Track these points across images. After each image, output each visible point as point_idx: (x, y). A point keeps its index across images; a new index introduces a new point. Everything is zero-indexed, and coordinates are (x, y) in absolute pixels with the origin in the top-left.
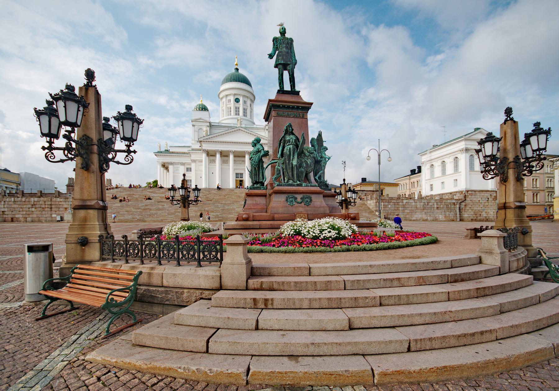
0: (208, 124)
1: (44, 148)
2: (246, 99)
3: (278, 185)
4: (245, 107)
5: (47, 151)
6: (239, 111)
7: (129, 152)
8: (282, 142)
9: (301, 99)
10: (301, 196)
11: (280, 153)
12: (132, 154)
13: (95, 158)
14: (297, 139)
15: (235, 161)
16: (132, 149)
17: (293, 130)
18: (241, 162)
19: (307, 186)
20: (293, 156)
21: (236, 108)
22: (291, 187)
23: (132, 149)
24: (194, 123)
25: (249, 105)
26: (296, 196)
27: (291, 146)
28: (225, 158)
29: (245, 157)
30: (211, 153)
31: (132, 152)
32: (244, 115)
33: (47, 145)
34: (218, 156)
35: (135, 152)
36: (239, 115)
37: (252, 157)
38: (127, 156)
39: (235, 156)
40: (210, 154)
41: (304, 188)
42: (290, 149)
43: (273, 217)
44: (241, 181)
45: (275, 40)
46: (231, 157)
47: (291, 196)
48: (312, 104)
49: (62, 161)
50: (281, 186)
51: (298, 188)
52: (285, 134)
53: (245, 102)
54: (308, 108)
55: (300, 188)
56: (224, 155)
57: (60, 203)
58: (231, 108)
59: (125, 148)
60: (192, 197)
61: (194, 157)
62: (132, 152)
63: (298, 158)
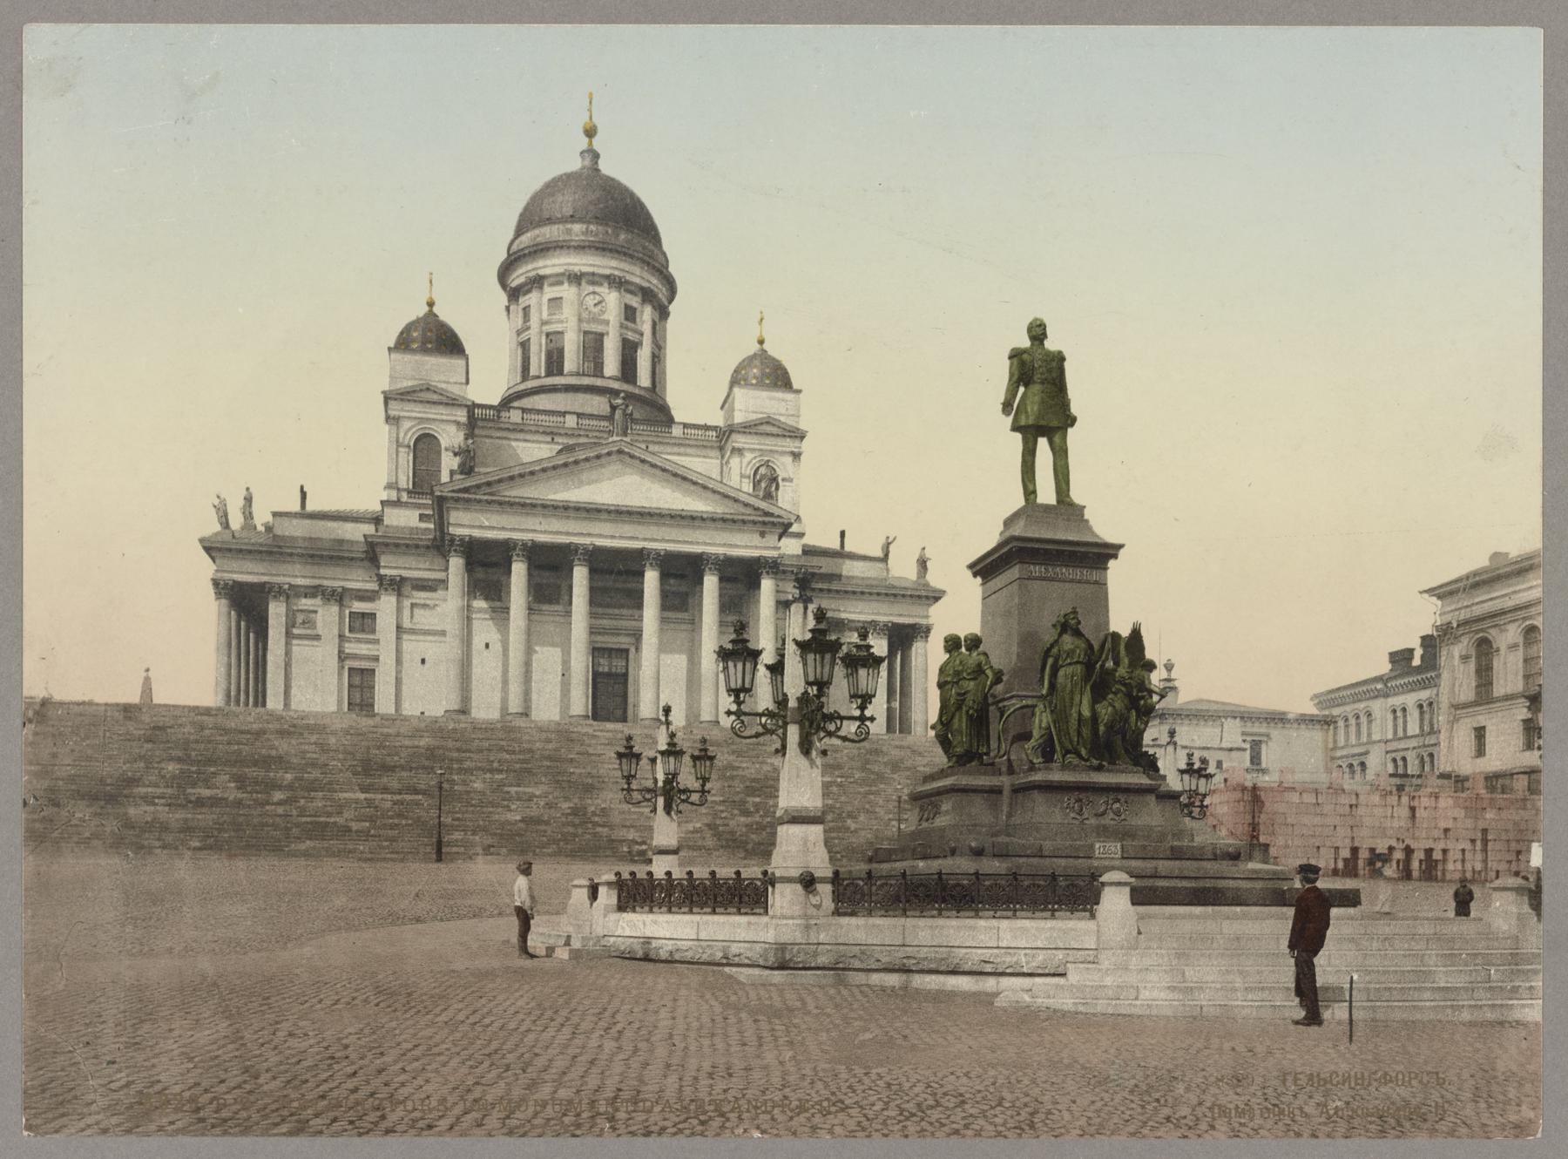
0: (462, 416)
1: (729, 713)
2: (634, 301)
5: (733, 717)
7: (862, 719)
9: (1093, 533)
14: (1091, 646)
16: (868, 713)
23: (868, 713)
24: (396, 409)
25: (647, 328)
33: (734, 708)
45: (1016, 355)
48: (1121, 546)
49: (757, 735)
52: (1060, 635)
53: (630, 314)
54: (1115, 556)
59: (857, 713)
61: (391, 566)
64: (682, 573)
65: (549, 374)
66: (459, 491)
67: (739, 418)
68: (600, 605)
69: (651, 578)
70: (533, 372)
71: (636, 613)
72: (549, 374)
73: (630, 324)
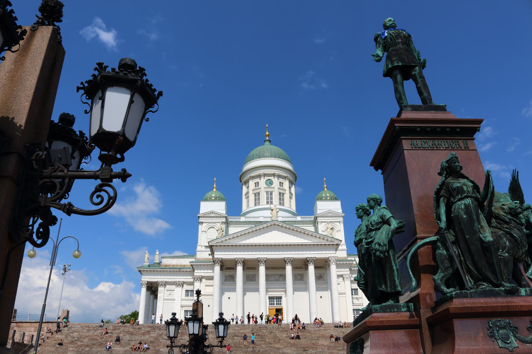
2: (281, 180)
3: (458, 296)
4: (281, 191)
6: (271, 198)
11: (444, 218)
12: (116, 182)
14: (476, 187)
15: (267, 276)
17: (461, 168)
18: (277, 277)
20: (479, 223)
22: (493, 299)
26: (515, 321)
27: (468, 201)
28: (251, 272)
29: (284, 268)
30: (227, 265)
31: (117, 176)
32: (280, 204)
34: (240, 269)
35: (124, 176)
36: (272, 203)
37: (361, 240)
38: (99, 189)
39: (267, 268)
40: (228, 267)
42: (467, 206)
44: (279, 311)
46: (262, 269)
50: (466, 296)
51: (509, 299)
53: (281, 184)
56: (250, 267)
58: (259, 193)
60: (211, 339)
62: (117, 176)
64: (301, 266)
65: (255, 205)
66: (219, 243)
68: (271, 281)
69: (289, 268)
70: (250, 206)
71: (284, 282)
72: (255, 205)
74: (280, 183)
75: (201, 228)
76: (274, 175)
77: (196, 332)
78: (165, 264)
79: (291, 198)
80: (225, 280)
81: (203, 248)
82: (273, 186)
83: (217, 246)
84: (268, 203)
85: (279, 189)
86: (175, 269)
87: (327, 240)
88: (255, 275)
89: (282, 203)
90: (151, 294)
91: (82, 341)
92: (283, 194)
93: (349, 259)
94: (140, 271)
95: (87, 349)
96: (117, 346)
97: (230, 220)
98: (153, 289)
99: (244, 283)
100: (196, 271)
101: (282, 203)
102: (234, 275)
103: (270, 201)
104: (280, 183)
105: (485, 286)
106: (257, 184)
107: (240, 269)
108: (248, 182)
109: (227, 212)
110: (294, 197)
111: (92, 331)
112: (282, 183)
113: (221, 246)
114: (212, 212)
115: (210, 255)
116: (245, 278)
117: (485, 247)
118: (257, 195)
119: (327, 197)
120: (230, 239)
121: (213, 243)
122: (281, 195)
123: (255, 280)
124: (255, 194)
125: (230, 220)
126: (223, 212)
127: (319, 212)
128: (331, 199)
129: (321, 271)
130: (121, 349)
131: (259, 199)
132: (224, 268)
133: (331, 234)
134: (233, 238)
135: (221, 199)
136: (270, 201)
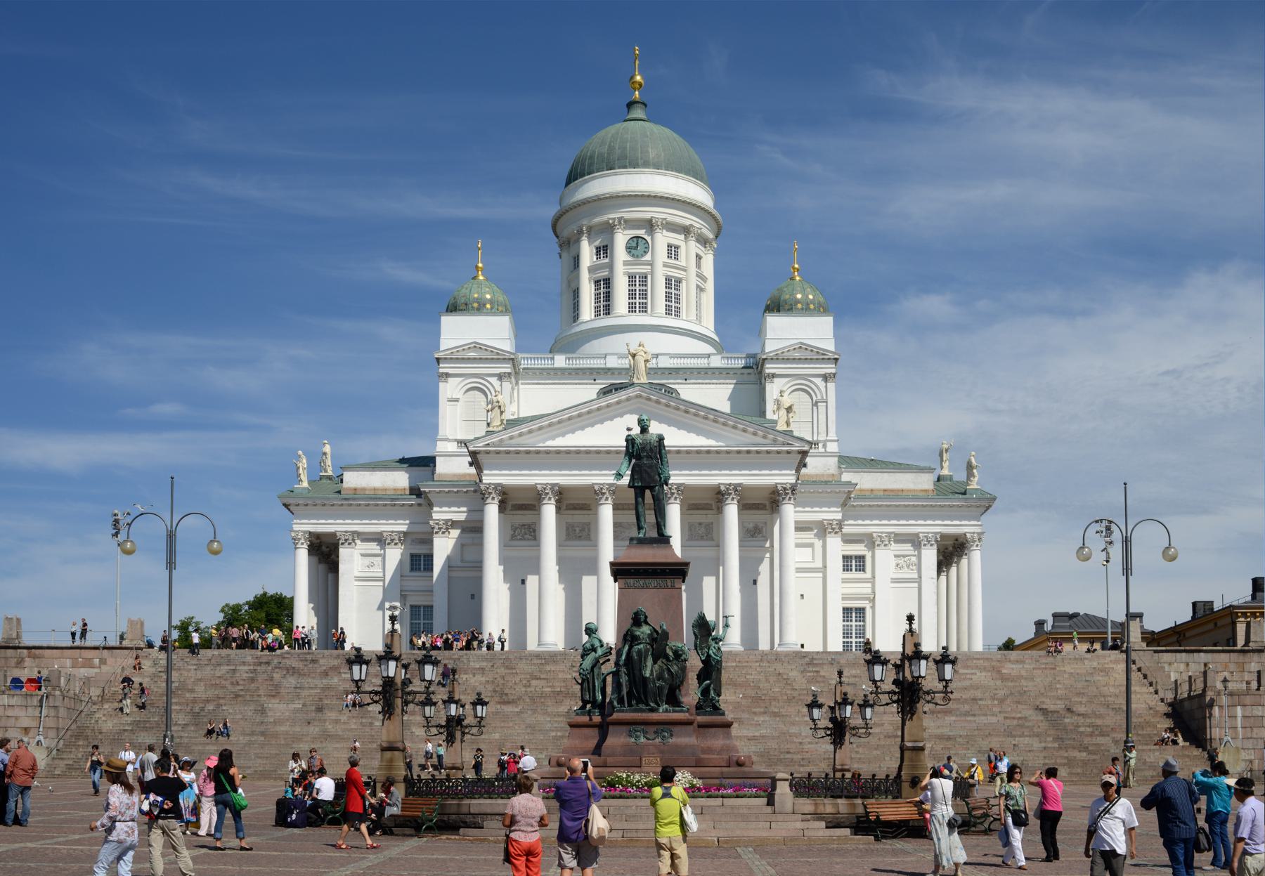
6: (644, 294)
8: (628, 638)
10: (654, 728)
13: (399, 702)
19: (667, 711)
21: (632, 278)
27: (641, 646)
28: (578, 517)
34: (549, 512)
41: (664, 713)
43: (605, 762)
47: (639, 728)
53: (673, 250)
55: (654, 716)
57: (10, 713)
58: (608, 282)
63: (655, 662)
66: (494, 445)
67: (771, 347)
72: (597, 314)
73: (672, 261)
74: (669, 246)
75: (449, 389)
76: (650, 225)
77: (453, 713)
78: (353, 486)
79: (700, 289)
80: (513, 537)
81: (452, 447)
82: (648, 257)
83: (488, 452)
84: (632, 309)
85: (665, 265)
86: (380, 499)
87: (775, 440)
88: (589, 524)
89: (673, 309)
90: (320, 562)
91: (192, 691)
92: (679, 281)
93: (847, 477)
94: (286, 506)
95: (211, 707)
96: (273, 701)
97: (524, 364)
98: (324, 548)
99: (560, 545)
100: (435, 509)
101: (673, 309)
102: (535, 524)
103: (639, 302)
104: (669, 246)
105: (642, 706)
106: (604, 250)
107: (549, 512)
108: (578, 241)
109: (519, 348)
110: (710, 286)
111: (209, 668)
112: (677, 247)
113: (498, 452)
114: (476, 346)
115: (471, 464)
116: (564, 536)
117: (645, 680)
118: (605, 286)
119: (798, 301)
120: (521, 435)
121: (479, 446)
122: (673, 284)
123: (588, 538)
124: (597, 282)
125: (524, 364)
126: (507, 346)
127: (771, 347)
128: (808, 309)
129: (757, 517)
130: (282, 706)
131: (608, 296)
132: (509, 507)
133: (788, 424)
134: (530, 432)
135: (497, 309)
136: (639, 302)
